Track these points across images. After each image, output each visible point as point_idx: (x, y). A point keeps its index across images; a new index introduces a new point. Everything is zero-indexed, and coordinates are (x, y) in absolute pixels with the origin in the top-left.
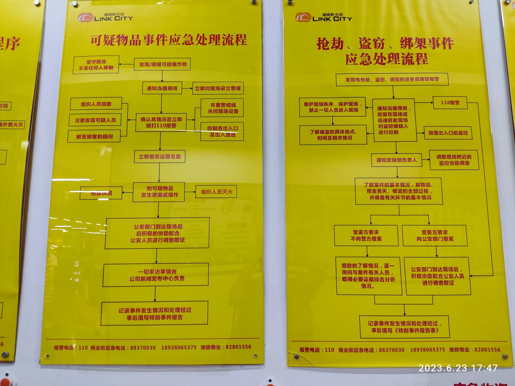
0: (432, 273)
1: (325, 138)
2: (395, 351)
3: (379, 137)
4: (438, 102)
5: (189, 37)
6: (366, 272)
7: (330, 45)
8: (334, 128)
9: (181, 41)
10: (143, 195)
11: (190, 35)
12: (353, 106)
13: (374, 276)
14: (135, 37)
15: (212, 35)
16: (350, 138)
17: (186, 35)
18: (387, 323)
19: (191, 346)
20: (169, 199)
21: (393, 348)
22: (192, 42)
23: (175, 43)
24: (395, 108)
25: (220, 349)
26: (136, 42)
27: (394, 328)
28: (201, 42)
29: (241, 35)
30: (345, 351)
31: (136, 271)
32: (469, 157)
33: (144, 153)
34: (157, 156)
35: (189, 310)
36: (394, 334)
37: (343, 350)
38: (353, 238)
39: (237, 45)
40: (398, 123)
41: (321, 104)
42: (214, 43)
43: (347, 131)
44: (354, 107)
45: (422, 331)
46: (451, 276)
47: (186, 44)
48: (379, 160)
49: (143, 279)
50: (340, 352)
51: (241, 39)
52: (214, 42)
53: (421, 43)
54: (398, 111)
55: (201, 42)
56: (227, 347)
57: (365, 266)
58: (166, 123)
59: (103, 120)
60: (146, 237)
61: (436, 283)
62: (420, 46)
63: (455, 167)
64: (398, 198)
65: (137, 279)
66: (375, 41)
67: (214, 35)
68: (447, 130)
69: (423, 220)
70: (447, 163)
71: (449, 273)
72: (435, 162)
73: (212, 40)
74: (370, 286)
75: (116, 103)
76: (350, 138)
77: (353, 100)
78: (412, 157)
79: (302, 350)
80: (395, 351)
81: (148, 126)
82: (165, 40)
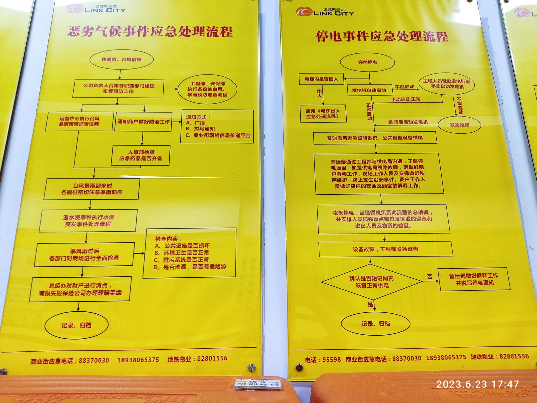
2: (98, 361)
19: (153, 358)
21: (210, 356)
25: (190, 361)
30: (187, 360)
37: (352, 359)
50: (348, 361)
56: (199, 358)
80: (98, 361)
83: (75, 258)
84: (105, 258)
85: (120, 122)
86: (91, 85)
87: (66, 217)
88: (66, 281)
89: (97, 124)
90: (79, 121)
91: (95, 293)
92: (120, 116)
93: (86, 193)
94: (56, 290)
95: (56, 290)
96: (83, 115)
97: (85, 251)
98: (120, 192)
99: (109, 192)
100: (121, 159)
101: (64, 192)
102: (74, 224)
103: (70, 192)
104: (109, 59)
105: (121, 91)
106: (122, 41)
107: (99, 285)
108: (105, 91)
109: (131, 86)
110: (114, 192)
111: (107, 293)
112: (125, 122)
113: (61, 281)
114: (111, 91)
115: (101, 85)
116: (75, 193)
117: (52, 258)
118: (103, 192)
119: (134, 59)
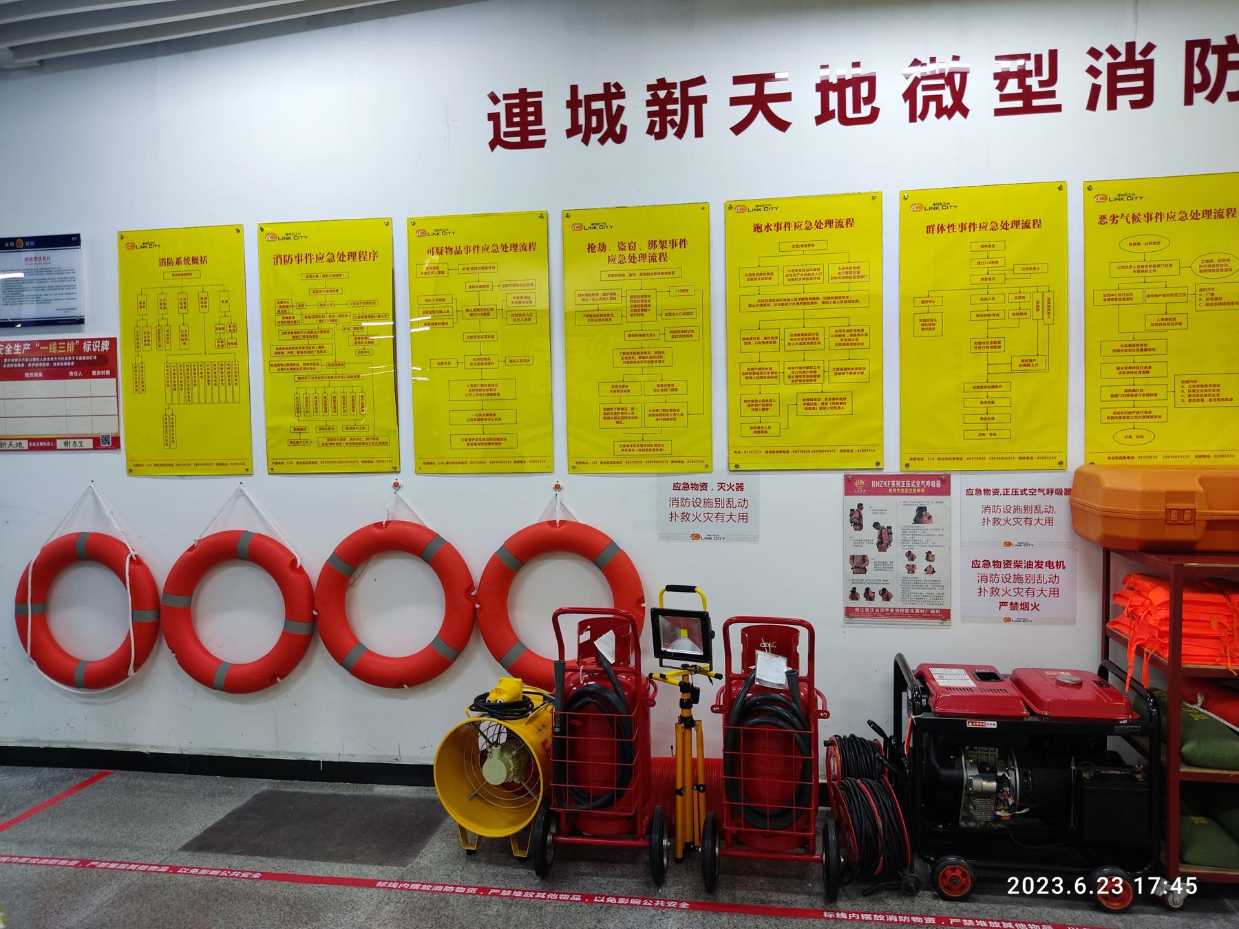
0: (662, 413)
1: (593, 320)
3: (630, 319)
4: (673, 290)
6: (619, 413)
7: (597, 249)
8: (600, 313)
10: (471, 364)
12: (613, 296)
13: (624, 416)
14: (458, 248)
16: (610, 320)
18: (631, 446)
20: (488, 366)
24: (642, 296)
26: (458, 252)
27: (635, 448)
31: (471, 415)
32: (693, 331)
33: (470, 335)
34: (478, 337)
35: (505, 439)
36: (636, 453)
38: (611, 391)
40: (644, 308)
41: (590, 295)
43: (608, 315)
44: (613, 296)
45: (654, 450)
46: (675, 415)
48: (630, 336)
49: (475, 420)
51: (532, 246)
53: (663, 244)
54: (644, 299)
57: (618, 409)
58: (483, 312)
59: (441, 312)
60: (475, 393)
61: (664, 419)
62: (662, 247)
63: (682, 339)
64: (642, 362)
65: (471, 420)
66: (629, 244)
68: (678, 311)
69: (659, 377)
70: (676, 337)
71: (673, 413)
72: (669, 336)
74: (621, 422)
75: (448, 299)
76: (610, 320)
77: (613, 291)
78: (653, 332)
79: (577, 463)
81: (471, 315)
83: (1128, 395)
84: (1148, 395)
85: (1148, 296)
86: (1123, 267)
87: (1118, 368)
88: (1124, 410)
89: (1131, 299)
90: (1118, 297)
91: (1144, 417)
92: (1148, 292)
93: (1130, 350)
94: (1118, 416)
95: (1118, 416)
96: (1123, 292)
97: (1134, 390)
98: (1154, 350)
99: (1146, 350)
100: (1152, 325)
101: (1114, 351)
102: (1124, 373)
103: (1118, 350)
104: (1134, 244)
105: (1146, 271)
106: (1143, 226)
107: (1146, 412)
108: (1135, 271)
109: (1154, 266)
110: (1150, 350)
111: (1152, 417)
112: (1152, 296)
113: (1120, 410)
114: (1139, 271)
115: (1131, 267)
116: (1122, 351)
117: (1112, 396)
118: (1142, 350)
119: (1154, 243)
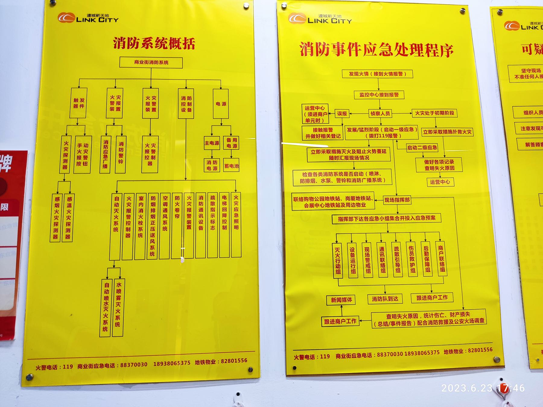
5: (386, 46)
9: (378, 51)
11: (387, 44)
15: (413, 44)
17: (383, 44)
22: (391, 53)
23: (371, 53)
28: (402, 52)
29: (432, 45)
39: (428, 56)
42: (416, 54)
47: (384, 55)
52: (416, 52)
55: (402, 52)
67: (415, 45)
73: (414, 50)
82: (358, 49)
